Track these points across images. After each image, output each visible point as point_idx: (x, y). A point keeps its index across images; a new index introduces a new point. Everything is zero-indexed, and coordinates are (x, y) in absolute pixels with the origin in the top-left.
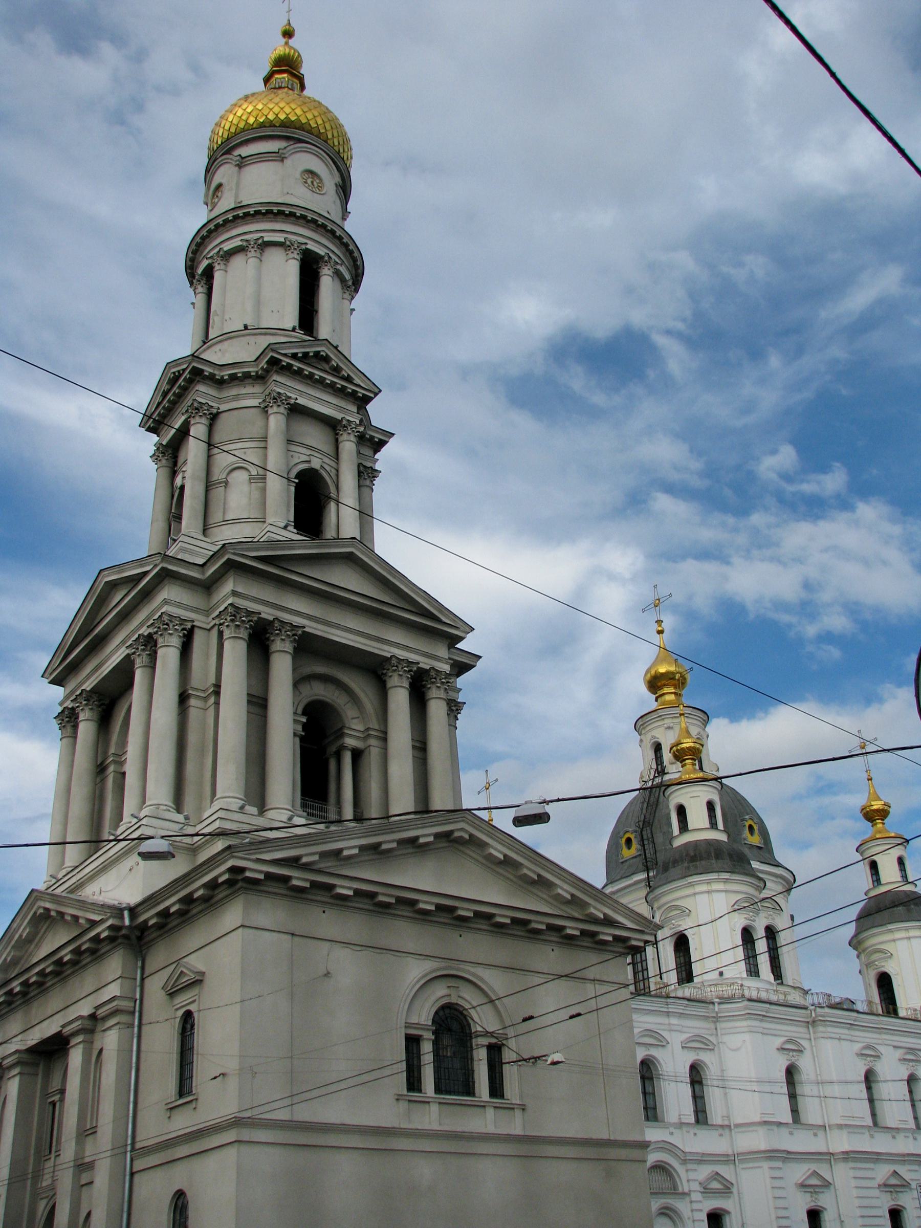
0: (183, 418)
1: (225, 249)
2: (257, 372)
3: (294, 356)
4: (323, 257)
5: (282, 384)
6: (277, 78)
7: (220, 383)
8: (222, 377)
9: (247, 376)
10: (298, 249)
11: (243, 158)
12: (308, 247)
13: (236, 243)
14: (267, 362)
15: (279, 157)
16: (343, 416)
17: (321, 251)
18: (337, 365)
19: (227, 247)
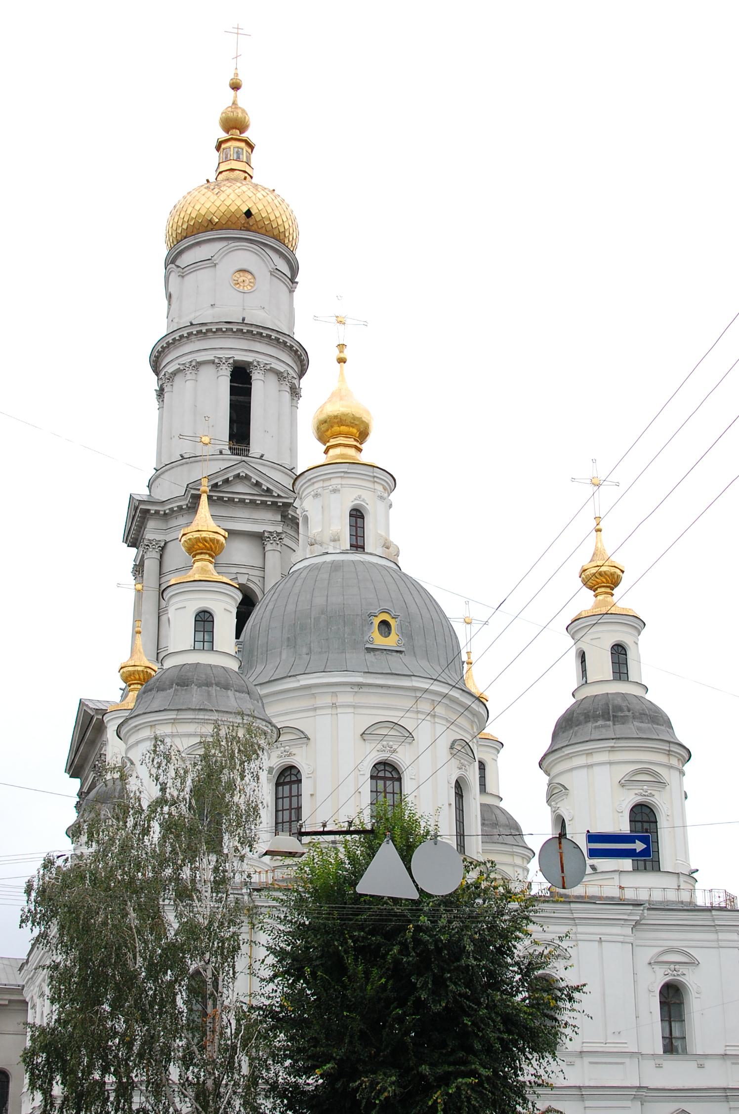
2: (187, 505)
3: (216, 485)
4: (249, 364)
6: (224, 149)
8: (165, 511)
9: (180, 508)
10: (226, 364)
11: (183, 269)
12: (237, 358)
14: (191, 497)
15: (210, 262)
17: (248, 358)
19: (171, 369)
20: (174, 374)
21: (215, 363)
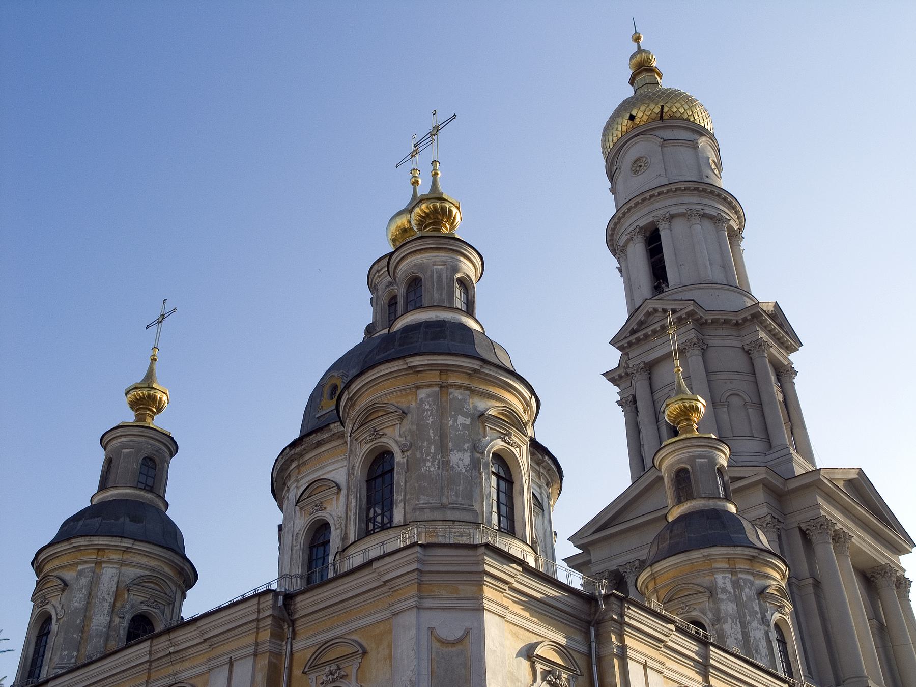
1: (672, 213)
8: (706, 320)
13: (682, 209)
19: (674, 210)
20: (672, 217)
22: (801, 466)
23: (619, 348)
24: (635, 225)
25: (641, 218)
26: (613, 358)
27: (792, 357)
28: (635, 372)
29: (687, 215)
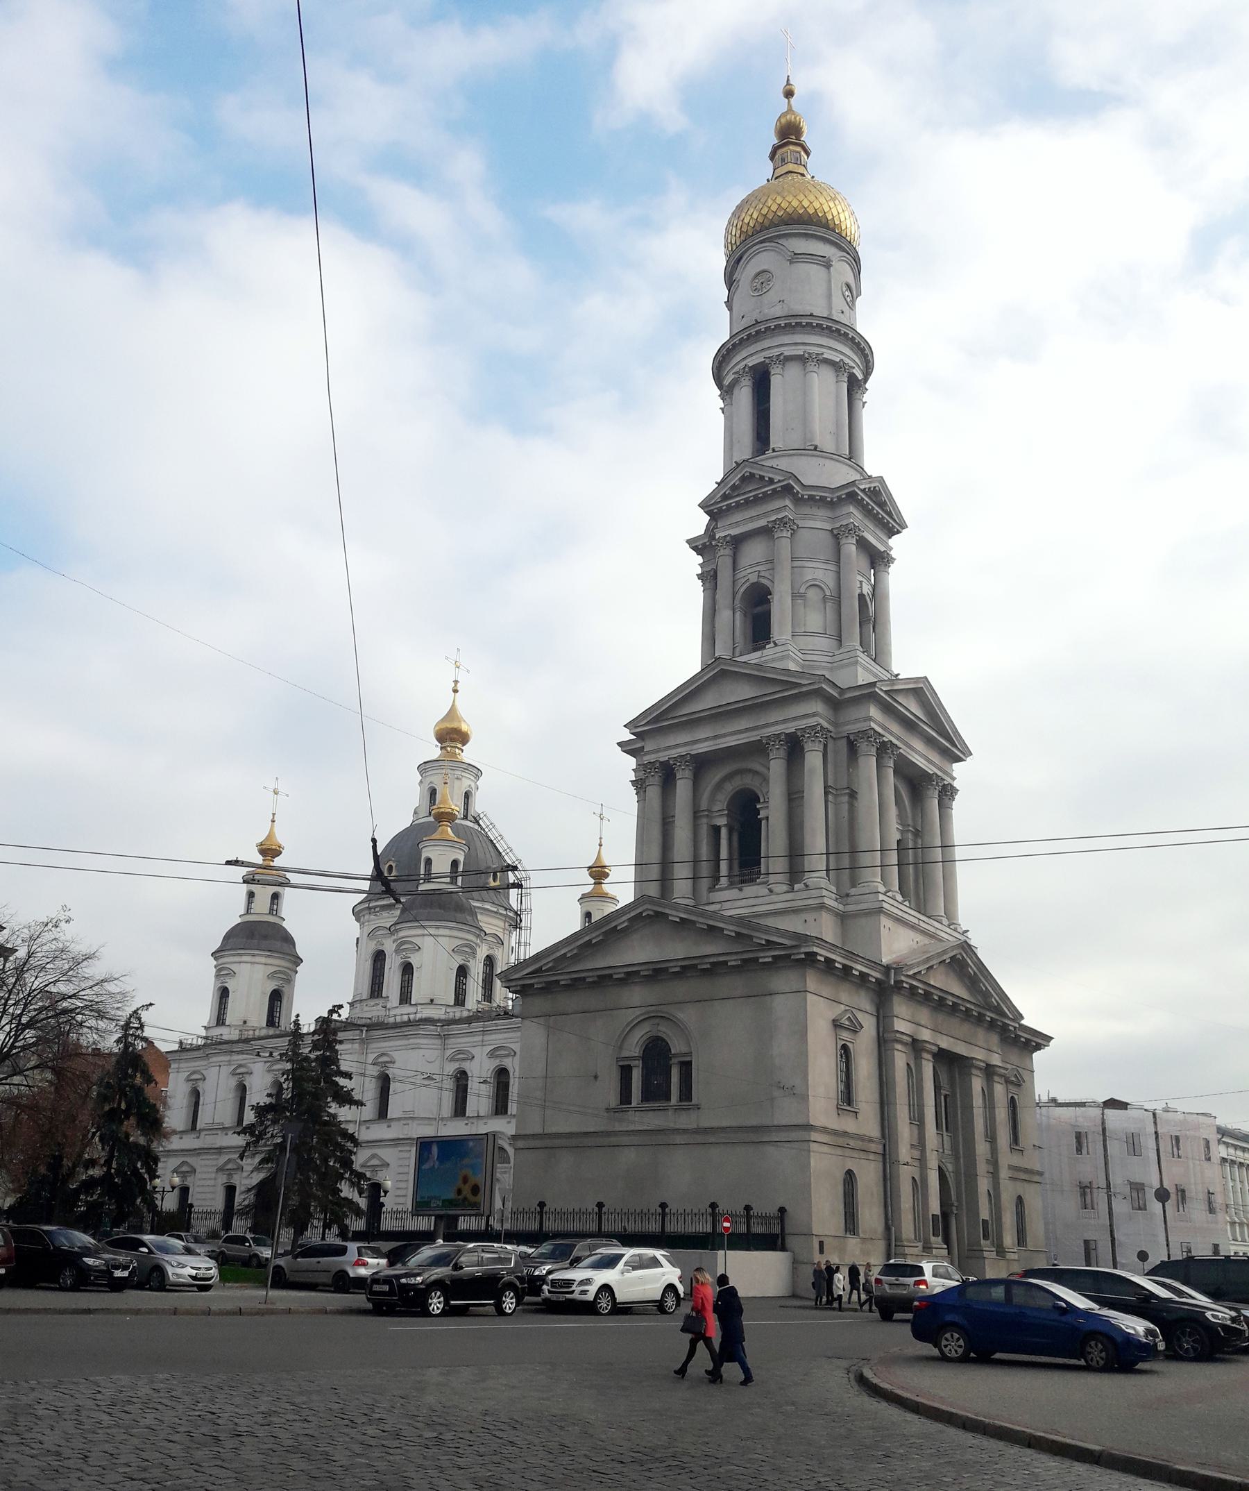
0: (762, 523)
1: (786, 353)
5: (854, 516)
7: (798, 500)
8: (802, 496)
9: (823, 499)
11: (795, 254)
12: (854, 371)
13: (799, 351)
16: (885, 549)
18: (885, 500)
19: (788, 351)
21: (837, 367)
22: (866, 669)
23: (706, 512)
24: (743, 364)
25: (752, 356)
26: (699, 523)
27: (894, 541)
28: (720, 545)
29: (802, 359)
